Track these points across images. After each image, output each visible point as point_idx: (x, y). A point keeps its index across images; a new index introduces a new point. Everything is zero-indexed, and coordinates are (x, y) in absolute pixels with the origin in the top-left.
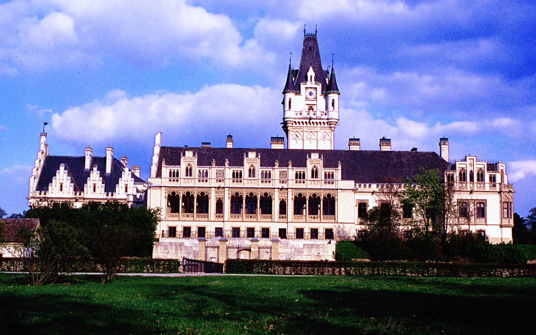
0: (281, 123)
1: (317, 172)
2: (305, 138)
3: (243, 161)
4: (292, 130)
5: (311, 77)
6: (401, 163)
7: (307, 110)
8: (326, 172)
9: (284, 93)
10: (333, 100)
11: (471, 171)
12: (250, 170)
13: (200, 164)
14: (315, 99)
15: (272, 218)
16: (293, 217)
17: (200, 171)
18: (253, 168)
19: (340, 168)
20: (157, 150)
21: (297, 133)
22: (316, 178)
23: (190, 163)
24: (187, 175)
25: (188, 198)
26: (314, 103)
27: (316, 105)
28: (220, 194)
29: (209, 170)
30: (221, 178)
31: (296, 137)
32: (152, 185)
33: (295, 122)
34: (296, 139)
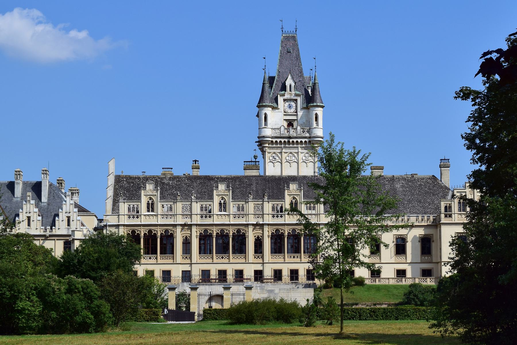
0: (256, 142)
2: (284, 161)
3: (212, 195)
4: (268, 151)
5: (290, 86)
6: (395, 190)
7: (286, 127)
10: (316, 114)
12: (220, 204)
13: (163, 197)
14: (295, 113)
15: (245, 259)
17: (163, 205)
18: (224, 201)
20: (111, 180)
24: (148, 211)
25: (150, 238)
26: (294, 118)
28: (188, 232)
31: (273, 159)
33: (272, 141)
34: (274, 162)
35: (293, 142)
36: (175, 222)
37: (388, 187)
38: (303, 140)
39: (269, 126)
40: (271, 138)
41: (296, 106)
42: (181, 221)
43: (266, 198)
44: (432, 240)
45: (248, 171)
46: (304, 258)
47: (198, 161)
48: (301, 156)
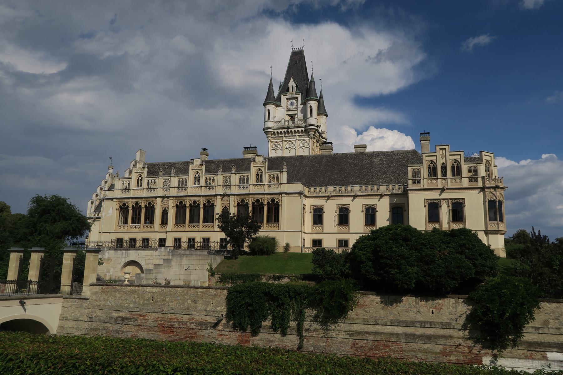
1: (261, 175)
9: (265, 104)
10: (311, 107)
11: (443, 163)
19: (285, 169)
21: (276, 144)
22: (260, 182)
27: (297, 114)
31: (276, 147)
32: (106, 198)
33: (274, 132)
35: (291, 131)
38: (300, 129)
39: (271, 119)
45: (246, 155)
46: (267, 227)
48: (299, 143)
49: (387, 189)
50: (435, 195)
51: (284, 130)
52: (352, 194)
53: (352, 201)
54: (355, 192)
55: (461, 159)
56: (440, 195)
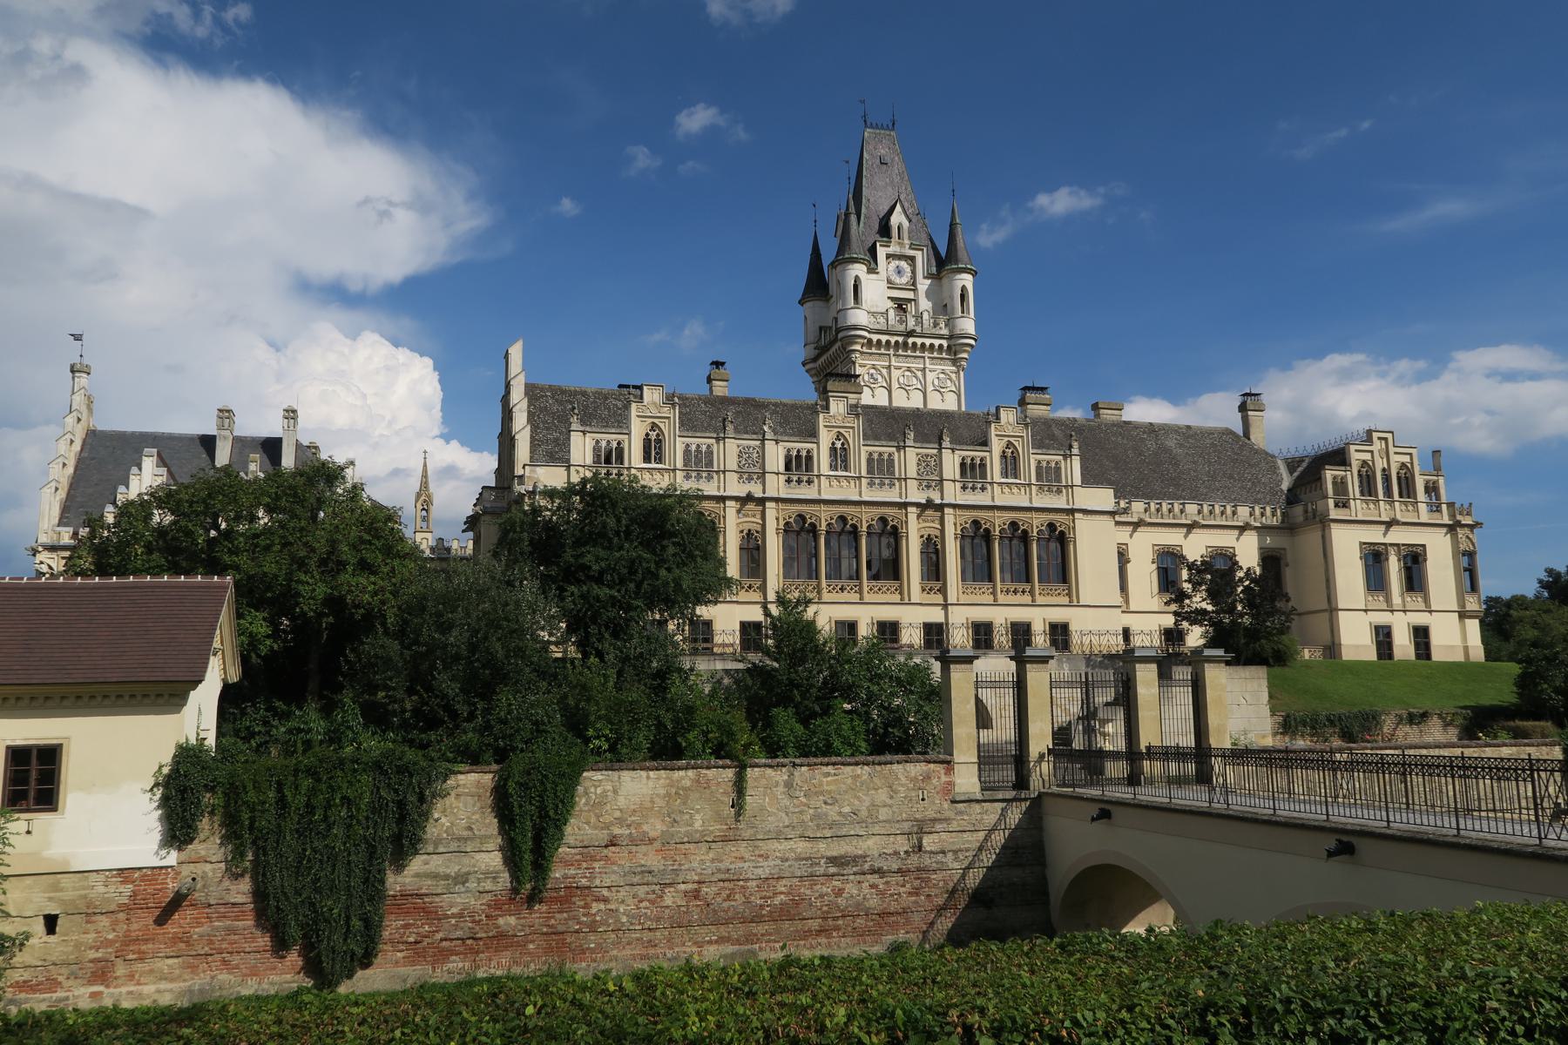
1: (1015, 459)
6: (1167, 450)
8: (1039, 462)
10: (964, 288)
12: (833, 449)
15: (901, 593)
16: (961, 592)
18: (843, 444)
19: (1075, 451)
21: (872, 371)
23: (656, 421)
26: (910, 295)
28: (753, 519)
29: (715, 445)
30: (754, 469)
33: (870, 341)
35: (914, 344)
36: (722, 490)
37: (1151, 444)
38: (937, 342)
40: (869, 332)
41: (914, 272)
42: (735, 488)
43: (946, 443)
44: (1282, 563)
47: (723, 364)
49: (1251, 515)
50: (1375, 535)
51: (896, 338)
52: (1184, 521)
53: (1186, 537)
54: (1189, 517)
55: (1412, 463)
56: (1385, 535)
